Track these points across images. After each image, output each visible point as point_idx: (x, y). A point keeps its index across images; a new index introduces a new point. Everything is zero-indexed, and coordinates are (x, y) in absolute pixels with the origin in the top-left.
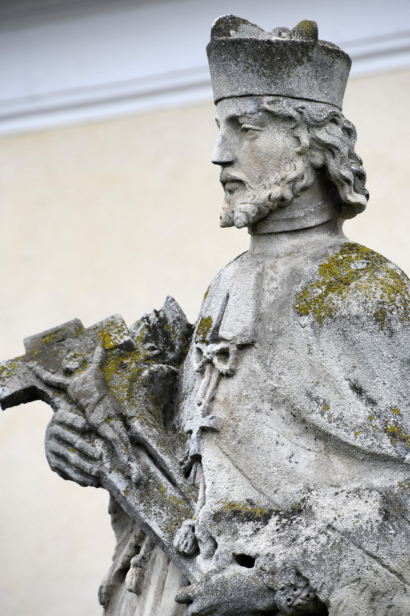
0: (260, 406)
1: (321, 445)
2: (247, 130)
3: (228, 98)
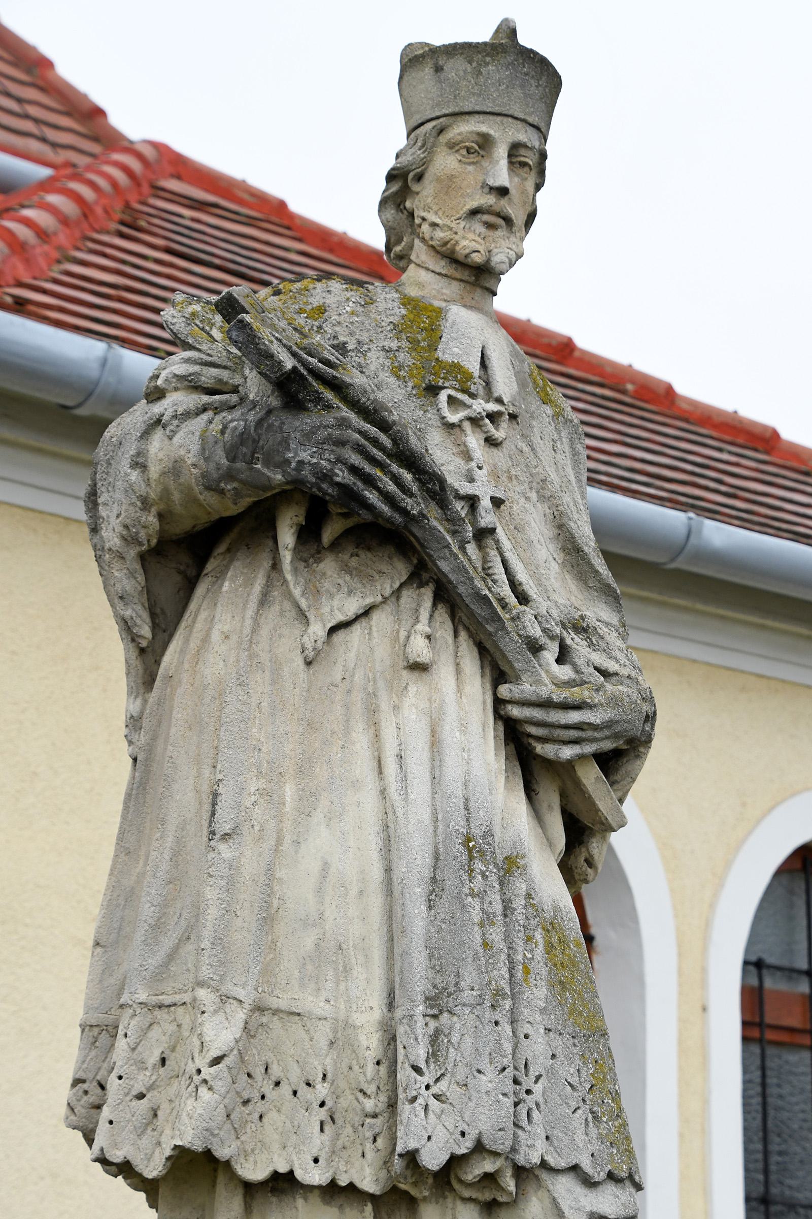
0: (529, 494)
1: (560, 557)
2: (524, 165)
3: (516, 118)
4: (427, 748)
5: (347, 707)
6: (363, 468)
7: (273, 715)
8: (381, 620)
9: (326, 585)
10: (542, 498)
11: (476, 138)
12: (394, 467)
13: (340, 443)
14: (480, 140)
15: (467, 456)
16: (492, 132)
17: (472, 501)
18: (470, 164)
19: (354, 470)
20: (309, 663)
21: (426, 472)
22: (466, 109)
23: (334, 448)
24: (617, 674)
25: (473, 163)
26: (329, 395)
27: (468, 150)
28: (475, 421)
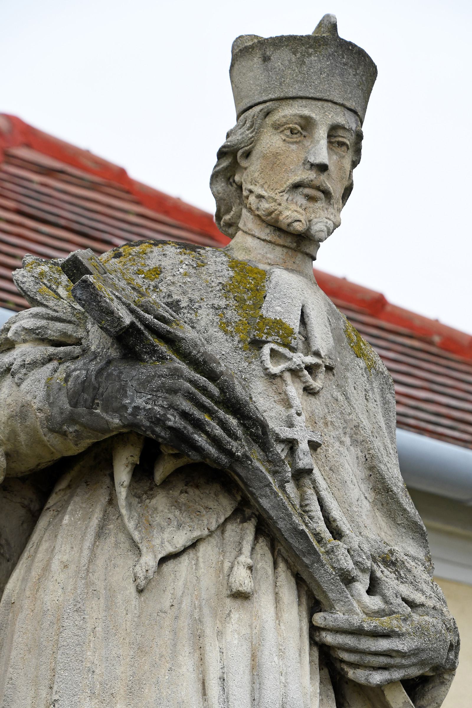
0: (343, 439)
1: (371, 496)
2: (341, 144)
3: (336, 103)
4: (247, 672)
5: (175, 632)
6: (193, 414)
7: (106, 639)
8: (206, 551)
9: (158, 519)
10: (355, 442)
11: (299, 120)
12: (221, 413)
13: (173, 391)
14: (303, 122)
15: (287, 403)
16: (313, 115)
17: (292, 445)
18: (293, 143)
19: (185, 415)
20: (140, 591)
21: (250, 418)
22: (290, 95)
23: (167, 395)
24: (423, 605)
25: (296, 142)
26: (163, 348)
27: (292, 131)
28: (295, 372)
